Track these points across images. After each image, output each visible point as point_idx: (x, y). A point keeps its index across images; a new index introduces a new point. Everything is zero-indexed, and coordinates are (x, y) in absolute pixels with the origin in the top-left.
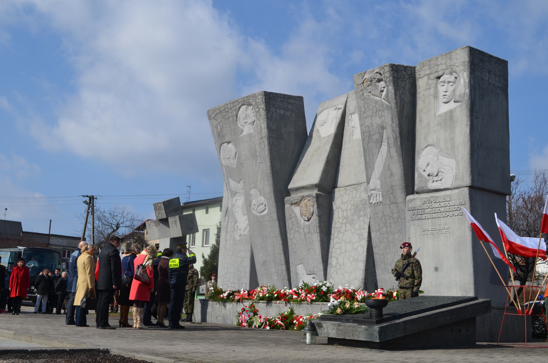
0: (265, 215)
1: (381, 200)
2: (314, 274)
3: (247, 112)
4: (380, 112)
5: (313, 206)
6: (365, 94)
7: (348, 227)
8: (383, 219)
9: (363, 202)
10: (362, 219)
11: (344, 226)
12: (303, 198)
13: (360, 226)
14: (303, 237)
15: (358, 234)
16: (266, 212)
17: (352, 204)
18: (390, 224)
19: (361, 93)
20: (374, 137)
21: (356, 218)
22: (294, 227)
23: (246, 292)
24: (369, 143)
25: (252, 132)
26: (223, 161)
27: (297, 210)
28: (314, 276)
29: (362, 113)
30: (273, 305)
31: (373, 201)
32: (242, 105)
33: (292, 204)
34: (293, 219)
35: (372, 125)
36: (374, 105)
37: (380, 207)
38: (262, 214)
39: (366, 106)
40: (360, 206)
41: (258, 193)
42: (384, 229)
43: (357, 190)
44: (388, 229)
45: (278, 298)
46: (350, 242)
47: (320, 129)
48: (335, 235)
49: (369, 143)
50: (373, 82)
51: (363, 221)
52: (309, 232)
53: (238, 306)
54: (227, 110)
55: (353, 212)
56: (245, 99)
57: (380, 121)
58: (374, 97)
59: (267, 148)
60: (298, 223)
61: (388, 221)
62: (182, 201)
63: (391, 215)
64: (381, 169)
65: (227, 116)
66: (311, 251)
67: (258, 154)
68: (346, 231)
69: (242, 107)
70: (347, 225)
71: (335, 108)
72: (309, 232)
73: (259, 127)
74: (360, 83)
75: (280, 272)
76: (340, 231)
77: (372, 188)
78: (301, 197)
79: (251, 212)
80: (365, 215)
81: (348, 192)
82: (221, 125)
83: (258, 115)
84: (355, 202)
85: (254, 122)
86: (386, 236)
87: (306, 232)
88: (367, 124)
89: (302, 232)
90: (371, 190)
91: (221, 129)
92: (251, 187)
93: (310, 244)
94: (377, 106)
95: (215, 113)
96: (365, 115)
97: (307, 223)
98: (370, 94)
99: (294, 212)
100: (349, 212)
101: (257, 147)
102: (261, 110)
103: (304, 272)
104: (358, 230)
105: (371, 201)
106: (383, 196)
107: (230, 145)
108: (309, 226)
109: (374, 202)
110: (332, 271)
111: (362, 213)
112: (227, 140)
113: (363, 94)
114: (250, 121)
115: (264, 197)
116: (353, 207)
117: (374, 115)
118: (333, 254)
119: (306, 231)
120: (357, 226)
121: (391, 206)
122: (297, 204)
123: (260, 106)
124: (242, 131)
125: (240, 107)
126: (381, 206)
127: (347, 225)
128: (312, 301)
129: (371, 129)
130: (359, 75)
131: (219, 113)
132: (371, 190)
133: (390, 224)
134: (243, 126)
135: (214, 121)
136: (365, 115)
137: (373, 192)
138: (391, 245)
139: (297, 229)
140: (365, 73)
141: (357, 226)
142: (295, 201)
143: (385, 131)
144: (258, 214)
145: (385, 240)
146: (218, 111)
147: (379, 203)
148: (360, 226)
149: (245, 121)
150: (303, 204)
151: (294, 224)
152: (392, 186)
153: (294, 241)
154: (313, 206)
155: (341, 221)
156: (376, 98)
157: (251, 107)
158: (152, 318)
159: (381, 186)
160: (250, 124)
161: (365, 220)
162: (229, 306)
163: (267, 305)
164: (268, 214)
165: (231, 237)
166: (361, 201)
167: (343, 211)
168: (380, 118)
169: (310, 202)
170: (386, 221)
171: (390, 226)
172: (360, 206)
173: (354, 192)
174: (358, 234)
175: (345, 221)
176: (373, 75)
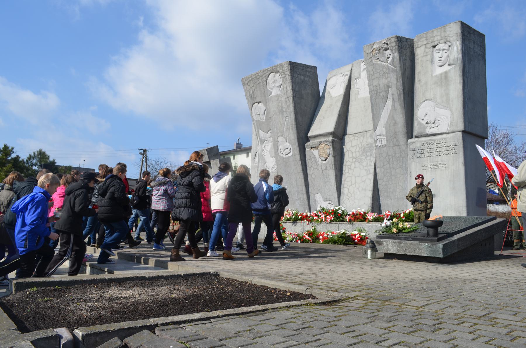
0: (290, 157)
1: (385, 143)
5: (330, 149)
6: (373, 61)
9: (369, 145)
10: (368, 158)
11: (353, 164)
12: (321, 143)
14: (321, 173)
19: (370, 60)
20: (381, 94)
21: (364, 158)
22: (313, 166)
24: (376, 99)
26: (254, 117)
27: (315, 152)
28: (330, 202)
31: (379, 144)
34: (313, 159)
35: (379, 85)
37: (385, 149)
38: (287, 156)
39: (374, 70)
41: (285, 140)
42: (388, 166)
43: (364, 137)
44: (391, 166)
45: (302, 219)
47: (330, 91)
48: (347, 171)
49: (376, 99)
51: (370, 160)
52: (326, 169)
54: (258, 77)
55: (361, 153)
57: (387, 81)
59: (292, 105)
60: (316, 162)
61: (391, 159)
65: (258, 82)
70: (356, 163)
72: (326, 169)
73: (285, 89)
75: (302, 199)
80: (371, 155)
81: (356, 138)
86: (389, 171)
88: (374, 84)
89: (320, 169)
91: (253, 93)
94: (384, 70)
96: (373, 77)
97: (324, 162)
98: (378, 61)
100: (358, 154)
101: (284, 104)
102: (287, 76)
103: (321, 199)
105: (377, 145)
106: (387, 140)
107: (260, 104)
108: (326, 164)
110: (345, 198)
111: (368, 154)
112: (258, 101)
114: (277, 84)
115: (289, 143)
117: (381, 77)
118: (345, 186)
119: (324, 168)
120: (365, 164)
121: (394, 148)
123: (286, 73)
124: (271, 93)
127: (356, 163)
128: (331, 221)
129: (378, 88)
134: (272, 89)
135: (247, 86)
136: (373, 77)
137: (379, 137)
138: (393, 178)
140: (374, 44)
142: (314, 146)
143: (390, 89)
146: (250, 79)
150: (321, 147)
152: (396, 132)
153: (313, 176)
154: (330, 149)
155: (351, 160)
157: (279, 74)
159: (386, 132)
161: (372, 159)
164: (292, 155)
166: (368, 145)
167: (352, 153)
168: (386, 79)
169: (327, 146)
170: (389, 159)
173: (362, 138)
175: (354, 160)
176: (381, 45)
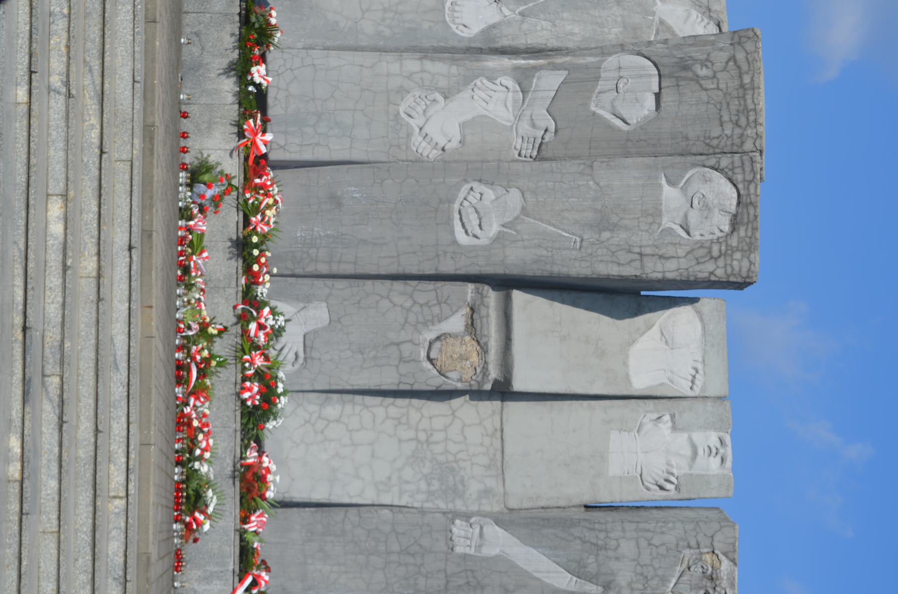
0: (452, 232)
1: (459, 550)
2: (305, 359)
3: (716, 211)
4: (641, 587)
5: (460, 380)
6: (687, 552)
7: (409, 448)
8: (417, 548)
9: (460, 487)
10: (423, 486)
11: (411, 434)
12: (484, 350)
13: (407, 482)
14: (392, 336)
15: (389, 478)
16: (461, 237)
17: (459, 456)
18: (406, 565)
19: (693, 543)
20: (592, 559)
21: (426, 471)
22: (416, 308)
23: (263, 150)
24: (583, 541)
25: (665, 220)
26: (612, 61)
27: (456, 323)
28: (301, 361)
29: (649, 535)
30: (233, 263)
31: (459, 528)
32: (739, 195)
33: (472, 309)
34: (436, 310)
35: (617, 559)
36: (660, 573)
37: (442, 546)
38: (457, 216)
39: (663, 550)
40: (451, 478)
41: (508, 219)
42: (395, 547)
43: (488, 467)
44: (394, 557)
45: (248, 270)
46: (373, 455)
47: (655, 331)
48: (393, 411)
49: (583, 541)
50: (709, 584)
51: (418, 491)
52: (401, 359)
53: (229, 127)
54: (743, 121)
55: (441, 458)
56: (752, 212)
57: (623, 584)
58: (677, 575)
59: (614, 271)
60: (425, 324)
61: (411, 560)
62: (467, 397)
63: (423, 570)
64: (521, 564)
65: (726, 118)
66: (359, 356)
67: (606, 235)
68: (400, 441)
69: (735, 195)
70: (412, 445)
71: (700, 366)
72: (401, 359)
73: (671, 251)
74: (716, 544)
75: (313, 251)
76: (400, 423)
77: (485, 529)
78: (486, 344)
79: (466, 181)
80: (430, 493)
81: (487, 441)
82: (709, 85)
83: (702, 252)
84: (461, 464)
85: (689, 234)
86: (382, 548)
87: (404, 347)
88: (623, 543)
89: (403, 336)
90: (481, 528)
91: (697, 79)
92: (527, 195)
93: (375, 358)
94: (654, 582)
95: (745, 67)
96: (643, 543)
97: (423, 354)
98: (685, 565)
99: (454, 313)
100: (438, 449)
101: (623, 235)
102: (710, 266)
103: (311, 327)
104: (400, 477)
105: (458, 522)
106: (465, 557)
107: (650, 102)
108: (416, 361)
109: (454, 530)
110: (312, 408)
111: (436, 485)
112: (666, 98)
113: (689, 547)
114: (694, 217)
115: (499, 238)
116: (451, 458)
117: (639, 570)
118: (348, 408)
119: (406, 349)
120: (408, 473)
121: (442, 575)
122: (472, 326)
123: (721, 262)
124: (671, 183)
125: (735, 185)
126: (445, 549)
127: (412, 445)
128: (244, 402)
129: (610, 553)
130: (734, 544)
131: (742, 86)
132: (481, 528)
133: (406, 565)
134: (684, 190)
135: (725, 56)
136: (643, 543)
137: (477, 530)
138: (361, 558)
139: (412, 318)
140: (733, 561)
141: (408, 473)
142: (478, 323)
143: (600, 589)
144: (456, 206)
145: (373, 544)
146: (747, 79)
147: (450, 543)
148: (407, 482)
149: (696, 202)
150: (471, 347)
151: (426, 309)
152: (483, 588)
153: (385, 304)
154: (460, 380)
155: (424, 424)
156: (674, 581)
157: (727, 228)
158: (210, 490)
159: (486, 559)
160: (686, 216)
161: (421, 497)
162: (229, 85)
163: (231, 240)
164: (455, 242)
165: (409, 77)
166: (462, 481)
167: (445, 429)
168: (630, 584)
169: (471, 372)
170: (413, 555)
171: (400, 564)
172: (451, 478)
173: (485, 461)
174: (389, 478)
175: (422, 436)
176: (725, 583)
